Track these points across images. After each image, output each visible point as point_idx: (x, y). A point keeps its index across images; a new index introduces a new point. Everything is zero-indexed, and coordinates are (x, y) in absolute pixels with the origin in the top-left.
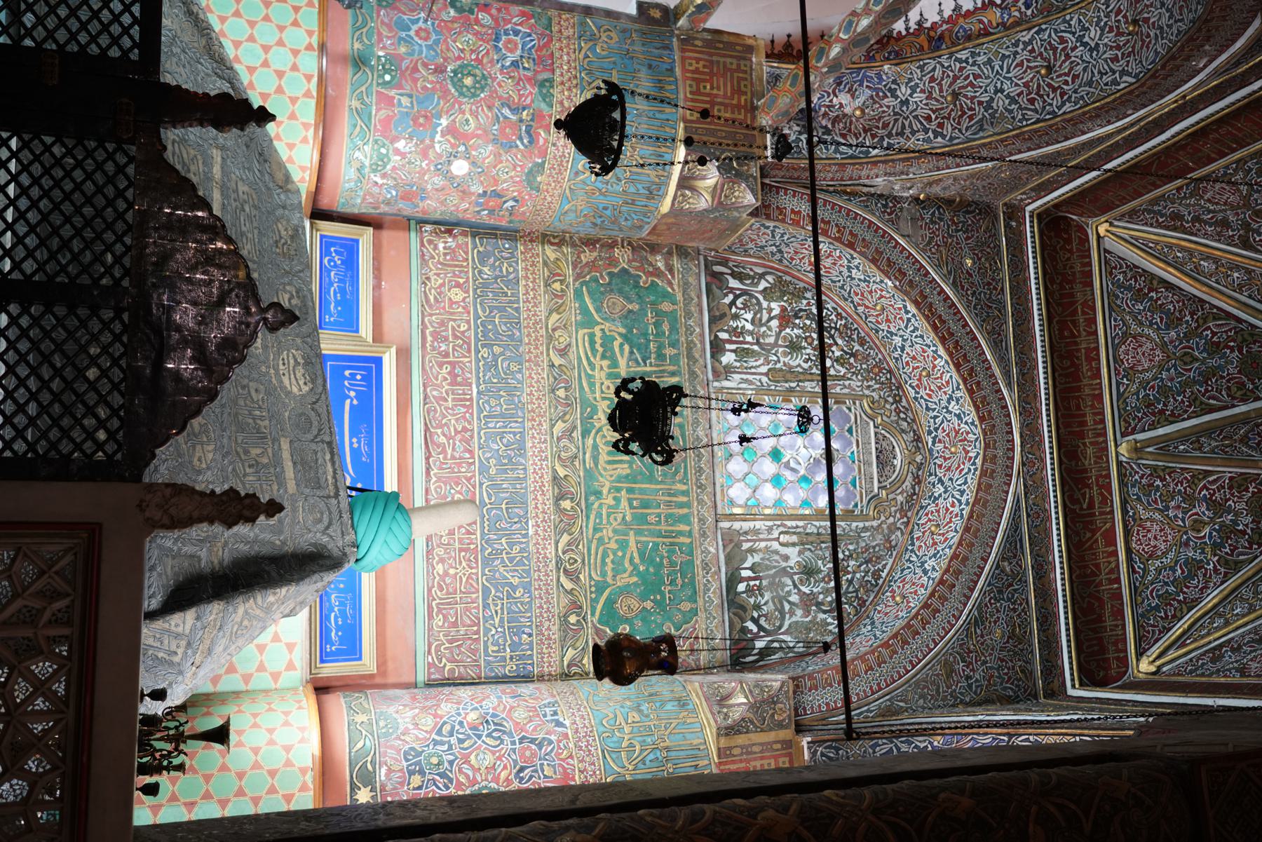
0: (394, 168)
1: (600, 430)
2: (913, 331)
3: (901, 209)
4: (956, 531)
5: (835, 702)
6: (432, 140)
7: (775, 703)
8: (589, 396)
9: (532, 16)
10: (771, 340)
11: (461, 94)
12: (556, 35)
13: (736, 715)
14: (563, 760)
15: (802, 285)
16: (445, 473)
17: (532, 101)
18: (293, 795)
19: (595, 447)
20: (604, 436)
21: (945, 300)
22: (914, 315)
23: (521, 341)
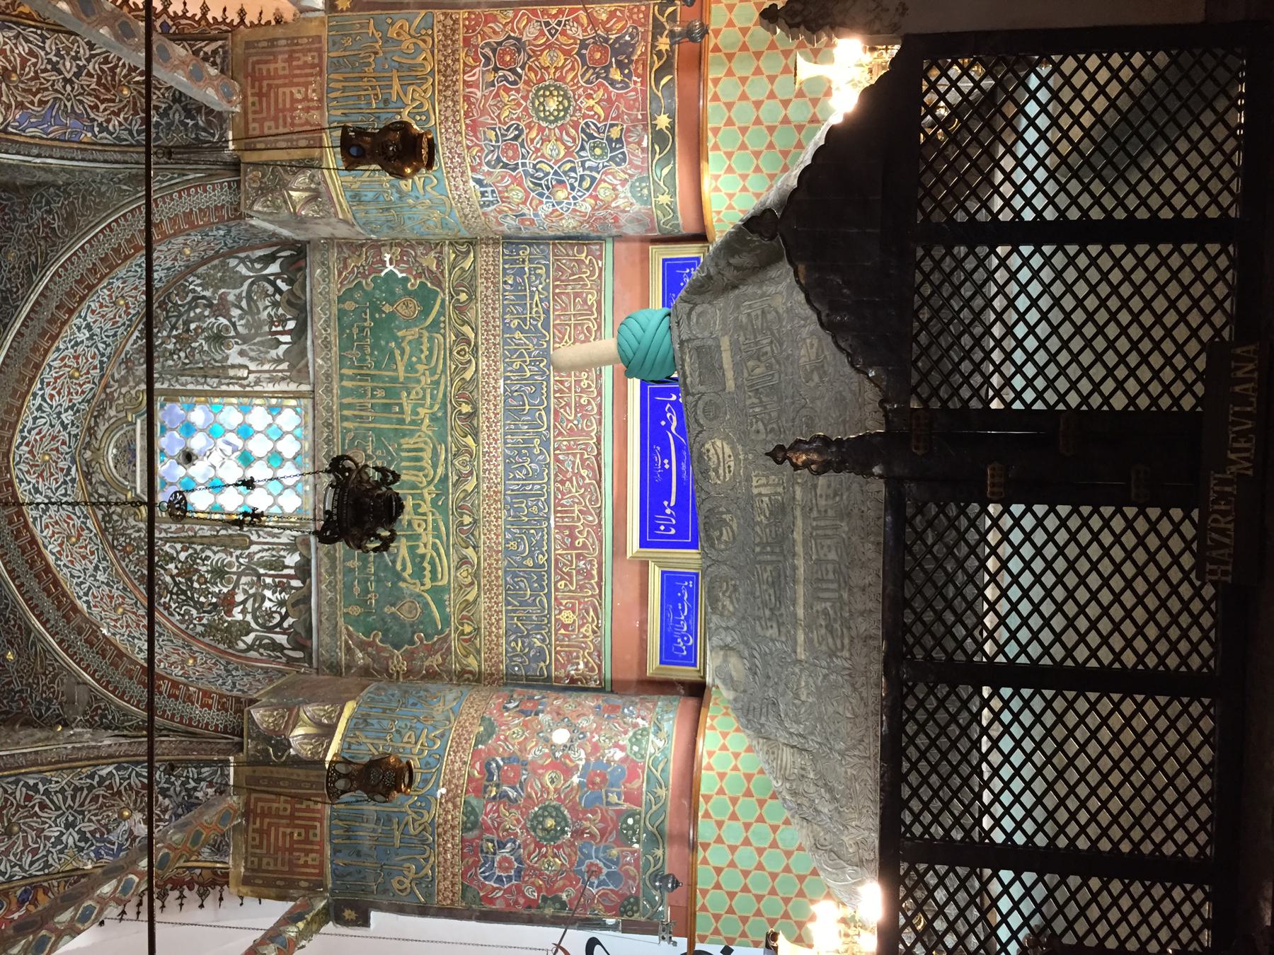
0: (626, 733)
1: (429, 483)
2: (82, 583)
3: (85, 713)
4: (50, 366)
5: (197, 192)
6: (587, 760)
7: (261, 188)
8: (438, 516)
9: (481, 899)
10: (244, 580)
11: (557, 809)
12: (458, 879)
13: (302, 179)
14: (476, 145)
15: (207, 640)
16: (582, 440)
17: (485, 806)
18: (726, 125)
19: (435, 466)
20: (426, 476)
21: (42, 613)
22: (80, 598)
23: (506, 572)
